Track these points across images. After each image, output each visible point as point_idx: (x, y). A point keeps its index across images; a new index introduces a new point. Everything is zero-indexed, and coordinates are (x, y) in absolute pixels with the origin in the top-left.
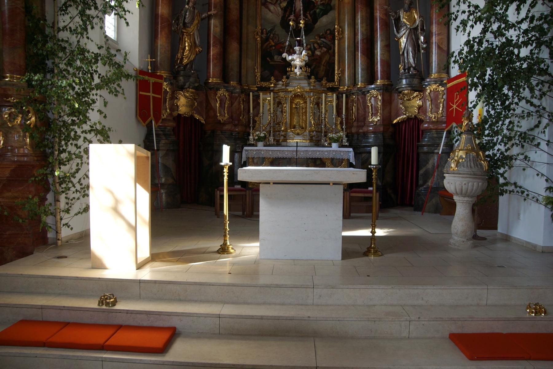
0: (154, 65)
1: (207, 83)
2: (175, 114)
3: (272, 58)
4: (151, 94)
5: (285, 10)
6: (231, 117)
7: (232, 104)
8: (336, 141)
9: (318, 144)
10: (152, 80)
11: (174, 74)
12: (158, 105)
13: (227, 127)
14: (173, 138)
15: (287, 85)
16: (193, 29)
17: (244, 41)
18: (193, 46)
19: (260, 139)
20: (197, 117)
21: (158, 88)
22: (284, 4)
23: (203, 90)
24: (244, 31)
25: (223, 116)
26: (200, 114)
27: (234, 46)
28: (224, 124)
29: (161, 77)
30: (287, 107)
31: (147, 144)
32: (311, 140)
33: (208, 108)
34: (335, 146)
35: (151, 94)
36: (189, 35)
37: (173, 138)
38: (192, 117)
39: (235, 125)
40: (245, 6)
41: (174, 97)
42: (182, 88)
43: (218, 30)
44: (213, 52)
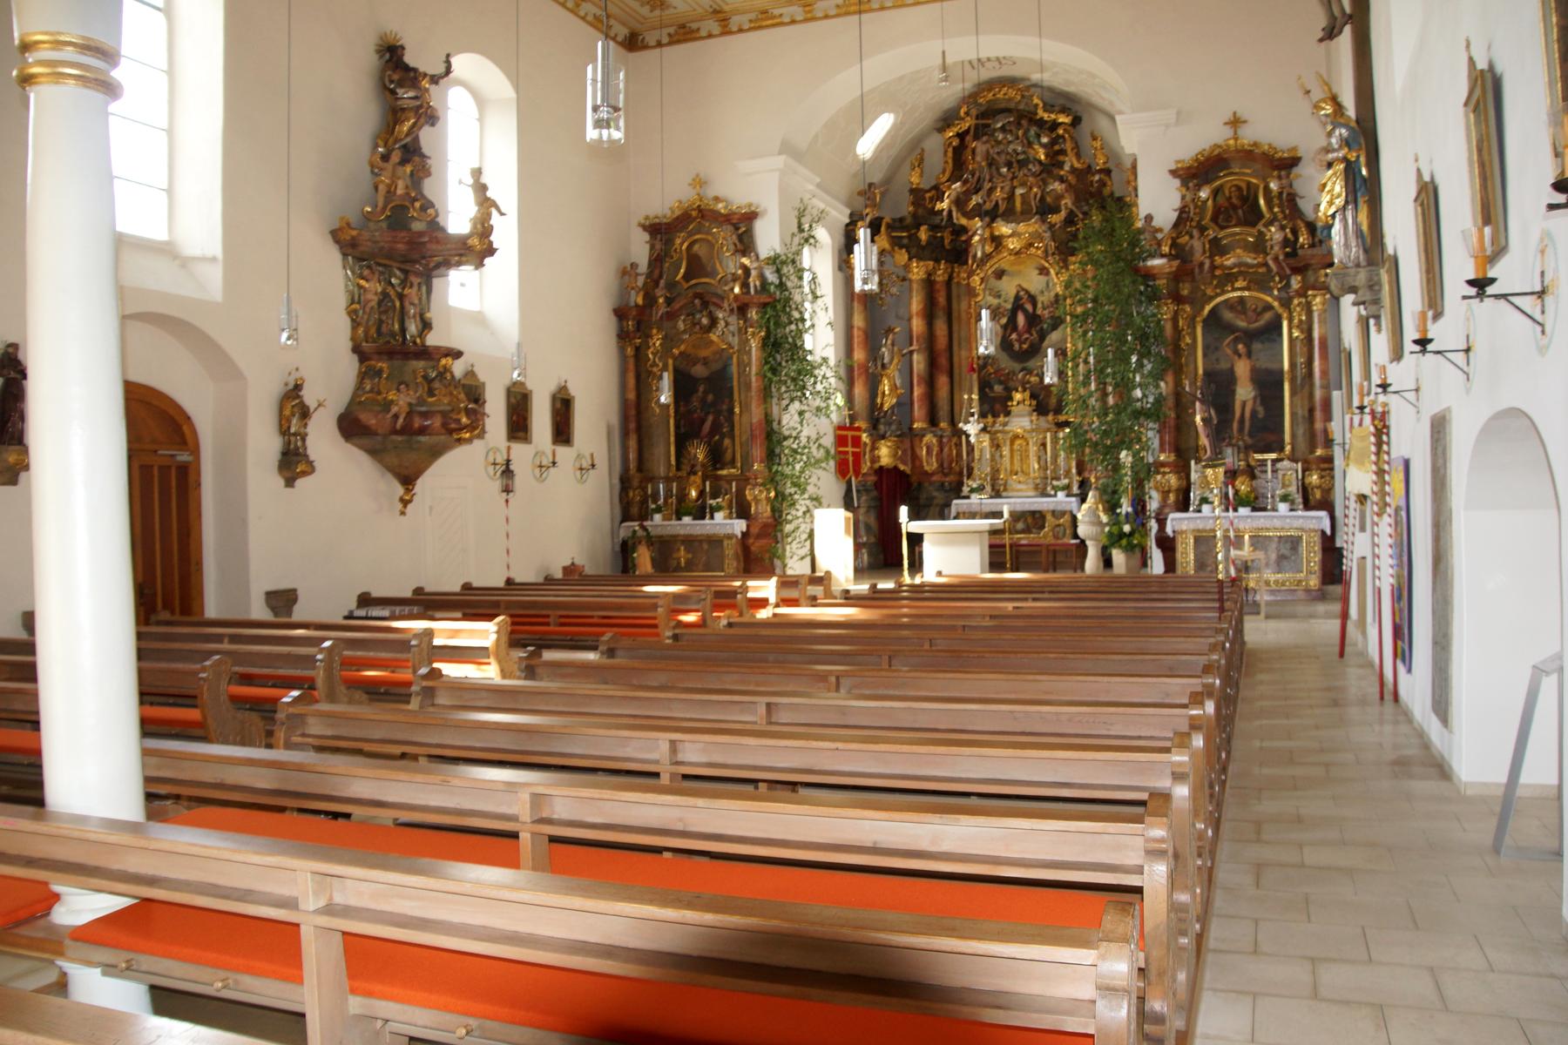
0: (852, 418)
1: (911, 429)
2: (877, 466)
3: (991, 388)
4: (850, 449)
5: (1005, 327)
6: (941, 465)
7: (941, 450)
8: (1063, 489)
9: (1044, 494)
10: (850, 433)
11: (874, 424)
12: (857, 457)
13: (934, 478)
14: (875, 493)
15: (1005, 424)
16: (893, 370)
17: (956, 371)
18: (894, 387)
19: (972, 491)
20: (902, 467)
21: (857, 441)
22: (1004, 321)
23: (907, 437)
24: (956, 359)
25: (931, 465)
26: (905, 463)
27: (942, 381)
28: (933, 474)
29: (859, 429)
30: (1006, 451)
31: (848, 504)
32: (1036, 487)
33: (915, 457)
34: (1061, 495)
35: (850, 449)
36: (888, 377)
37: (875, 493)
38: (896, 468)
39: (946, 475)
40: (955, 328)
41: (874, 448)
42: (883, 437)
43: (922, 366)
44: (917, 392)
